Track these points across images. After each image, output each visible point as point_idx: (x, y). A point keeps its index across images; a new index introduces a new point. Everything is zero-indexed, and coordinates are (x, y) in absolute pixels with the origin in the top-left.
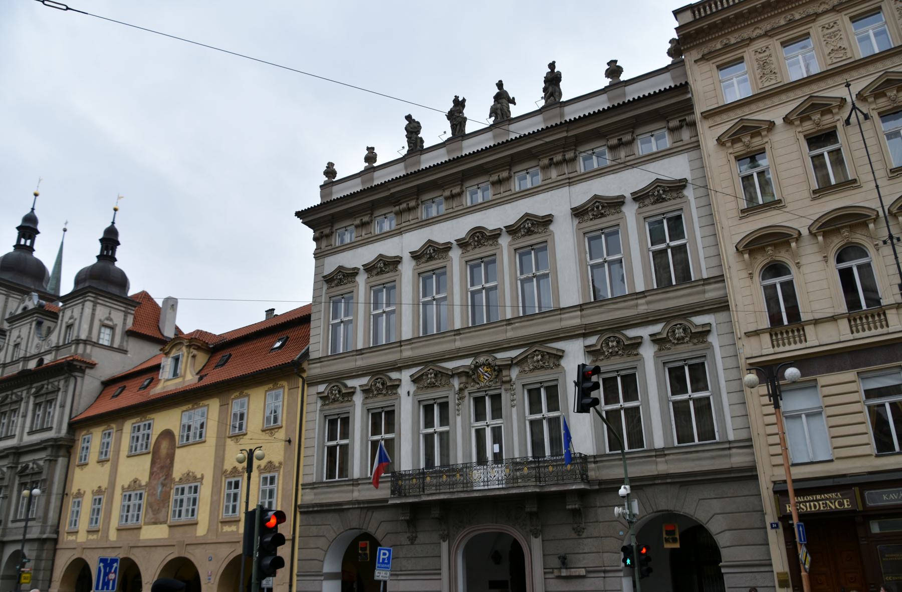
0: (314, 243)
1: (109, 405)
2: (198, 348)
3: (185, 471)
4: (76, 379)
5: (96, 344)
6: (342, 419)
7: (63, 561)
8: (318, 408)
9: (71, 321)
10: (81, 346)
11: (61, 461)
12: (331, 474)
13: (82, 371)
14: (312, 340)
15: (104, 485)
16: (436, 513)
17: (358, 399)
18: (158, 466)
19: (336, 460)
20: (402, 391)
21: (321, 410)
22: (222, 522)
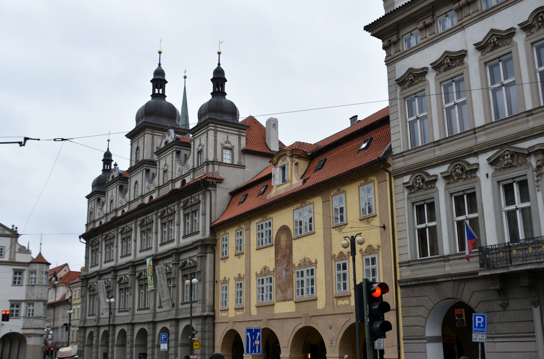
0: (384, 52)
1: (238, 210)
2: (299, 157)
4: (210, 192)
5: (221, 164)
6: (428, 205)
7: (220, 332)
8: (406, 197)
9: (201, 147)
10: (211, 166)
11: (209, 256)
12: (423, 252)
13: (215, 186)
14: (393, 138)
15: (243, 273)
16: (525, 282)
17: (441, 185)
18: (280, 255)
19: (427, 240)
20: (481, 174)
21: (408, 198)
22: (336, 297)
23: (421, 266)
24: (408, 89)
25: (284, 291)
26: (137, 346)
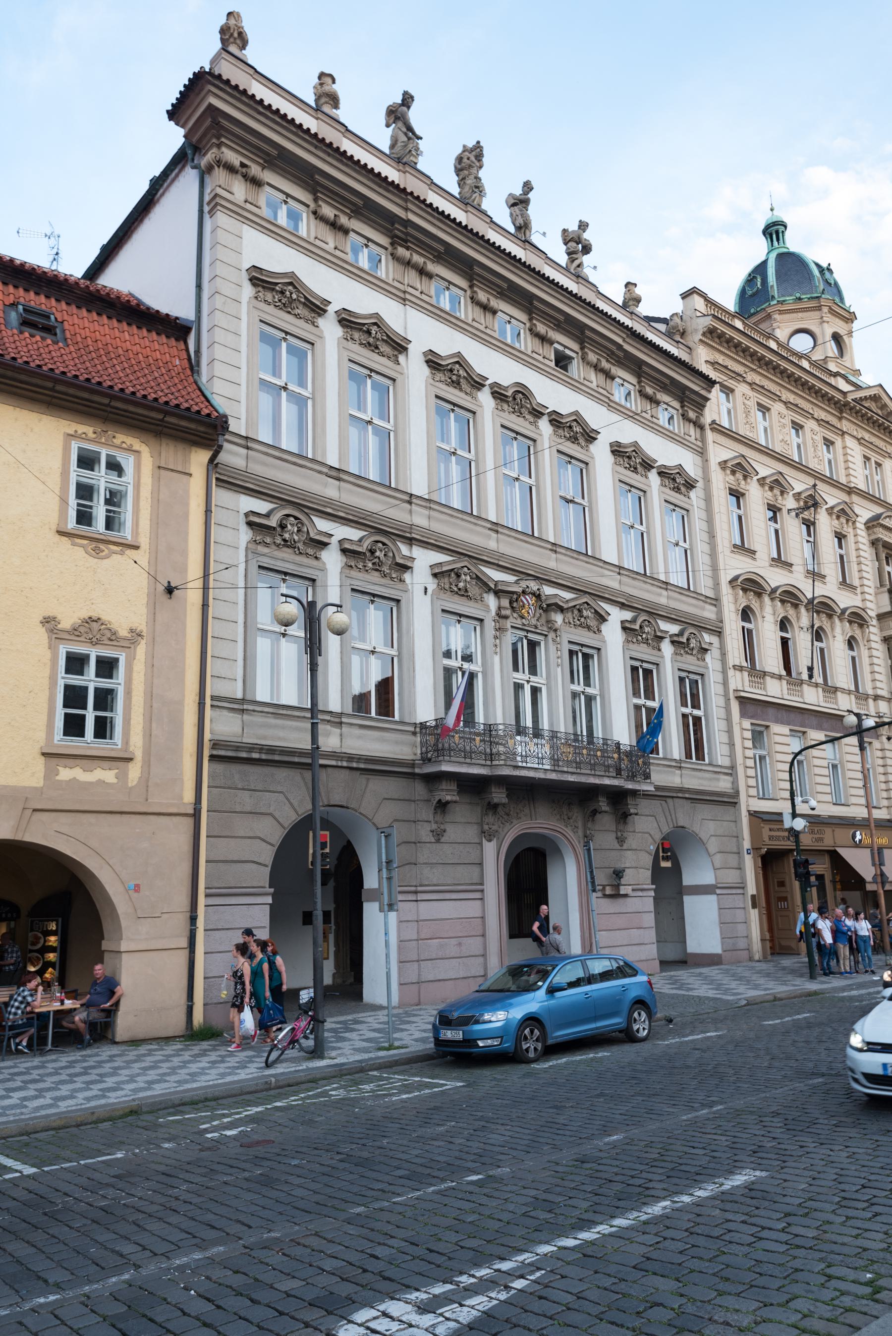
23: (272, 721)
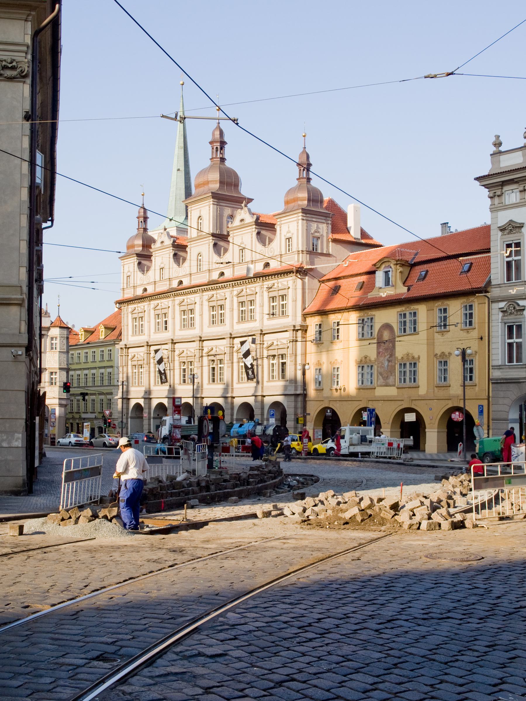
3: (405, 352)
7: (313, 409)
8: (500, 318)
12: (510, 360)
14: (492, 271)
23: (508, 370)
24: (507, 236)
25: (386, 378)
26: (131, 418)
